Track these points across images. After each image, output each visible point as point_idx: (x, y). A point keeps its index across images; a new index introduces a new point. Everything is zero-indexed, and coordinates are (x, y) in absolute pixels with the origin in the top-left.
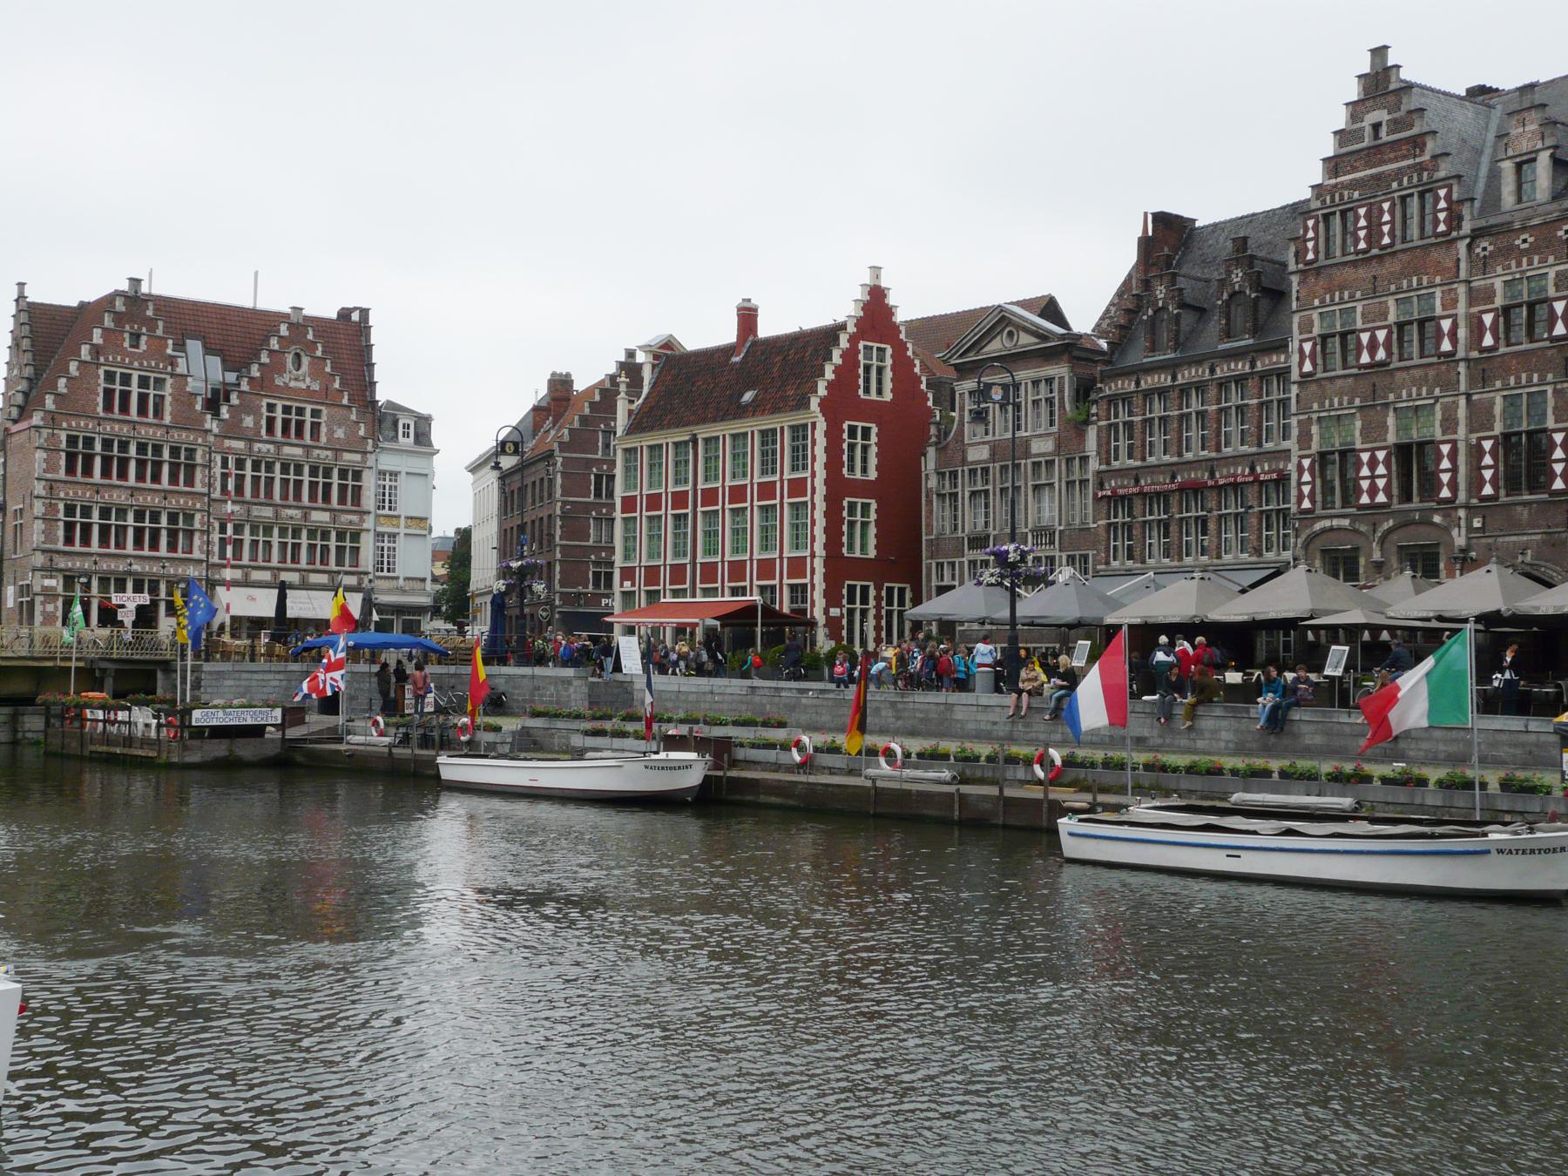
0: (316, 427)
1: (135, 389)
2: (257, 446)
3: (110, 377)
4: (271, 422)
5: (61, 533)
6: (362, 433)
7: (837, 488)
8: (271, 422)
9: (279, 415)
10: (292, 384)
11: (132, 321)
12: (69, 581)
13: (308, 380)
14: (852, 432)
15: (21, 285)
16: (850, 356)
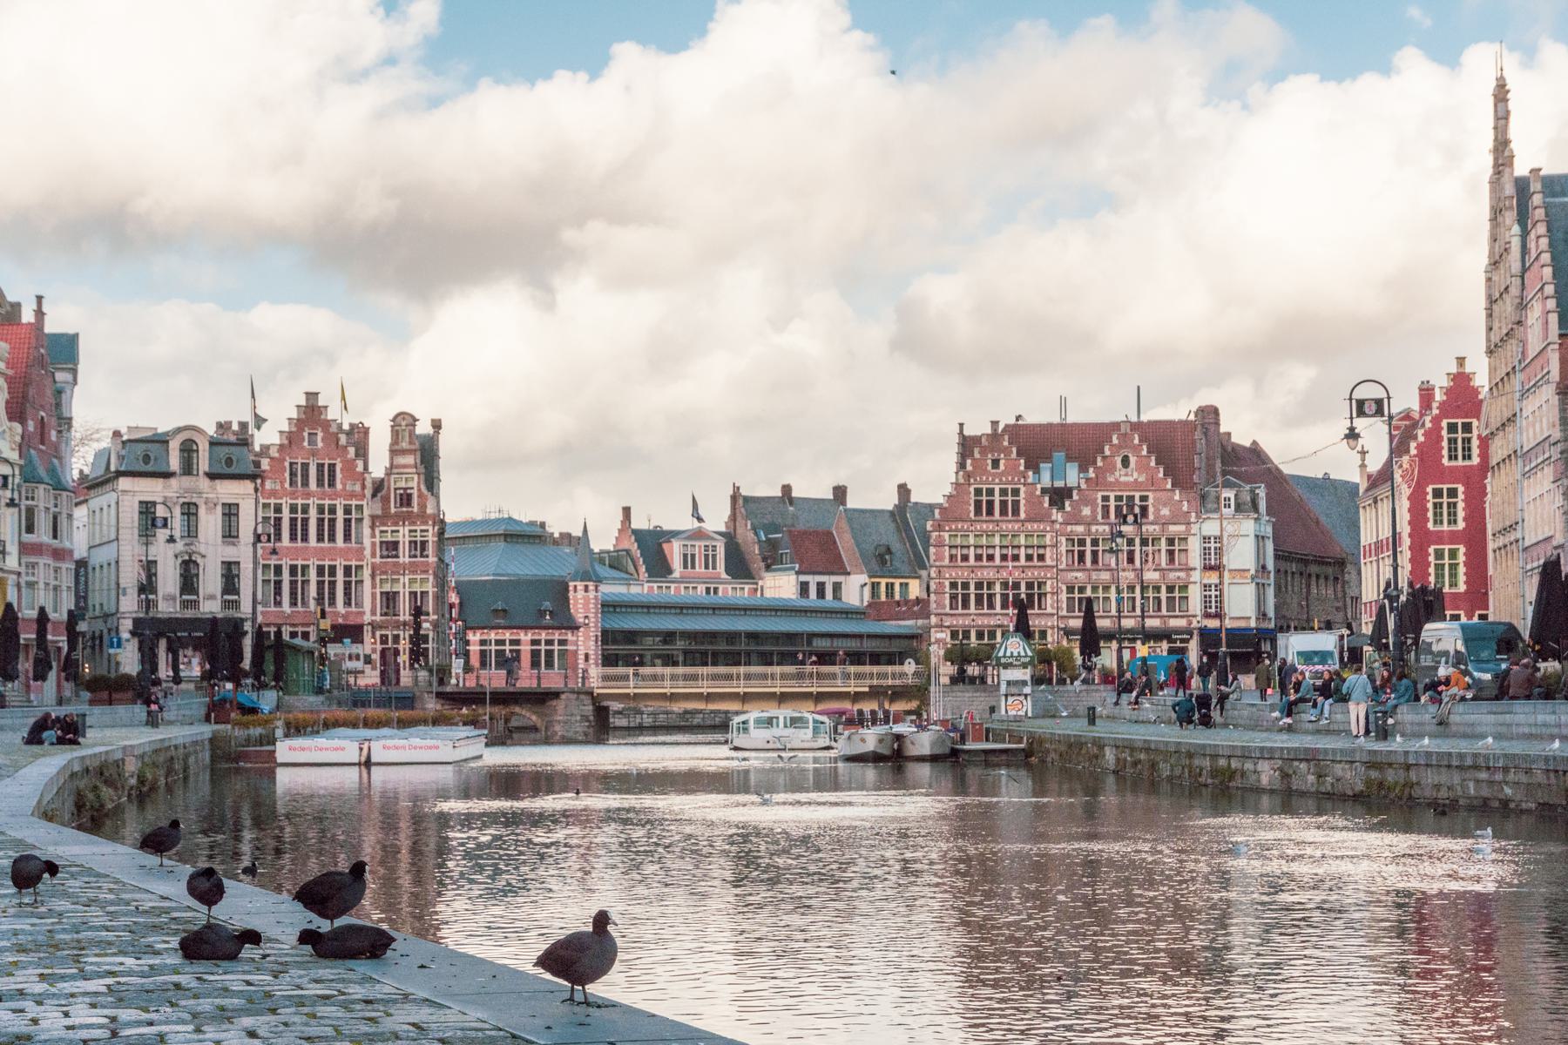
0: (1144, 509)
1: (997, 498)
2: (1094, 528)
3: (978, 492)
4: (1106, 509)
5: (947, 602)
6: (1185, 508)
7: (1421, 538)
8: (1106, 509)
9: (1112, 503)
10: (1123, 479)
11: (992, 451)
12: (954, 635)
13: (1135, 475)
14: (1438, 493)
15: (961, 425)
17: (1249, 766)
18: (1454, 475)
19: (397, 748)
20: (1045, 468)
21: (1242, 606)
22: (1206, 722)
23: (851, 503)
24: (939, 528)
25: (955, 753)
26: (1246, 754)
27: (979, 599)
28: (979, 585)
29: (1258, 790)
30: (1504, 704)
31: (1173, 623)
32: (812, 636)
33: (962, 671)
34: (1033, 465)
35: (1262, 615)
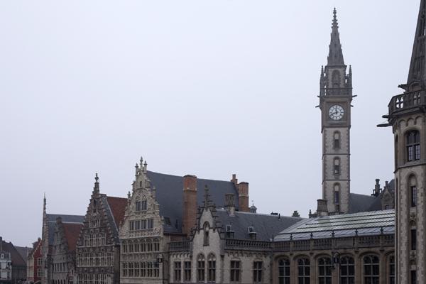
35: (8, 277)
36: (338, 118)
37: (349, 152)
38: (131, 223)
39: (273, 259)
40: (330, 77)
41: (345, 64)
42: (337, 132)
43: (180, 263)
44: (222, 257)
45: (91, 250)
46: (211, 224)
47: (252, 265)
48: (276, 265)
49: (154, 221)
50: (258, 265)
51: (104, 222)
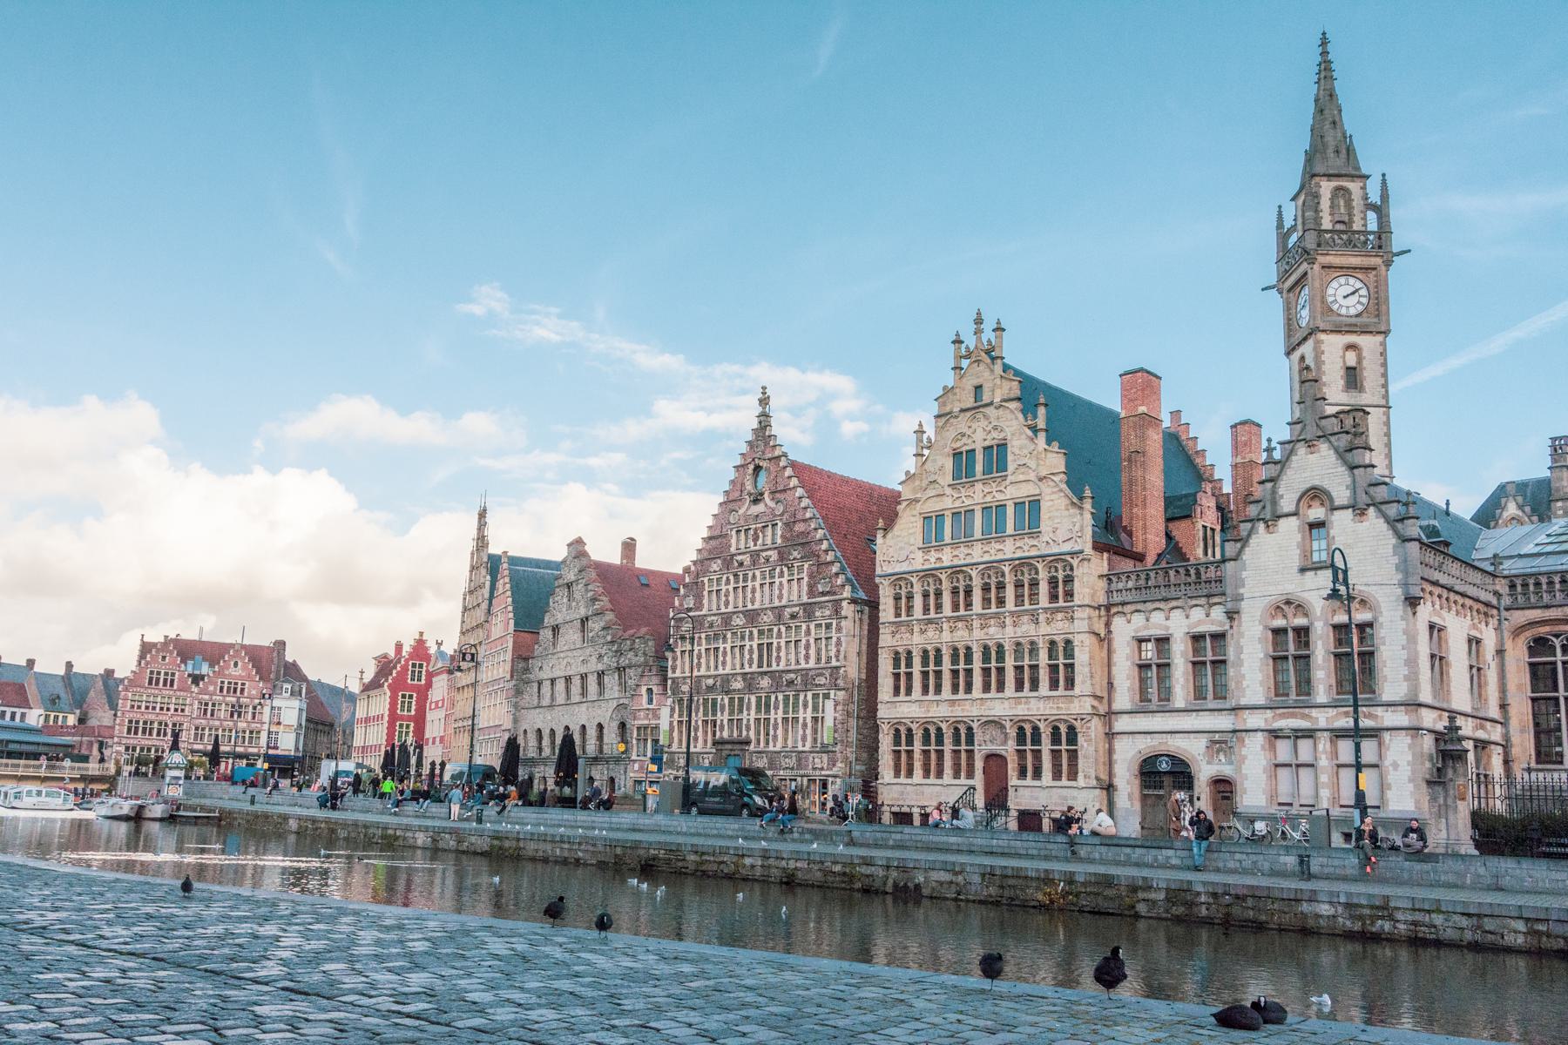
0: (242, 690)
16: (405, 668)
17: (409, 834)
18: (413, 688)
19: (707, 836)
20: (190, 663)
21: (287, 744)
22: (334, 807)
23: (36, 669)
24: (126, 689)
25: (172, 816)
26: (408, 828)
27: (1036, 738)
28: (145, 723)
29: (415, 848)
30: (543, 809)
31: (251, 750)
32: (8, 742)
33: (137, 769)
34: (184, 661)
35: (297, 749)
36: (1353, 311)
37: (1386, 396)
38: (933, 521)
39: (1506, 634)
40: (1325, 204)
41: (1364, 171)
42: (1351, 347)
43: (1163, 642)
44: (1412, 602)
45: (739, 621)
46: (1341, 495)
47: (1466, 647)
48: (1518, 655)
49: (1044, 506)
50: (1474, 642)
51: (799, 527)
